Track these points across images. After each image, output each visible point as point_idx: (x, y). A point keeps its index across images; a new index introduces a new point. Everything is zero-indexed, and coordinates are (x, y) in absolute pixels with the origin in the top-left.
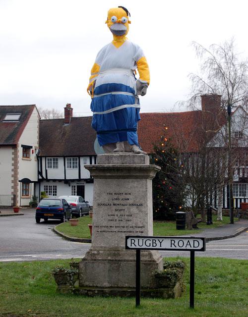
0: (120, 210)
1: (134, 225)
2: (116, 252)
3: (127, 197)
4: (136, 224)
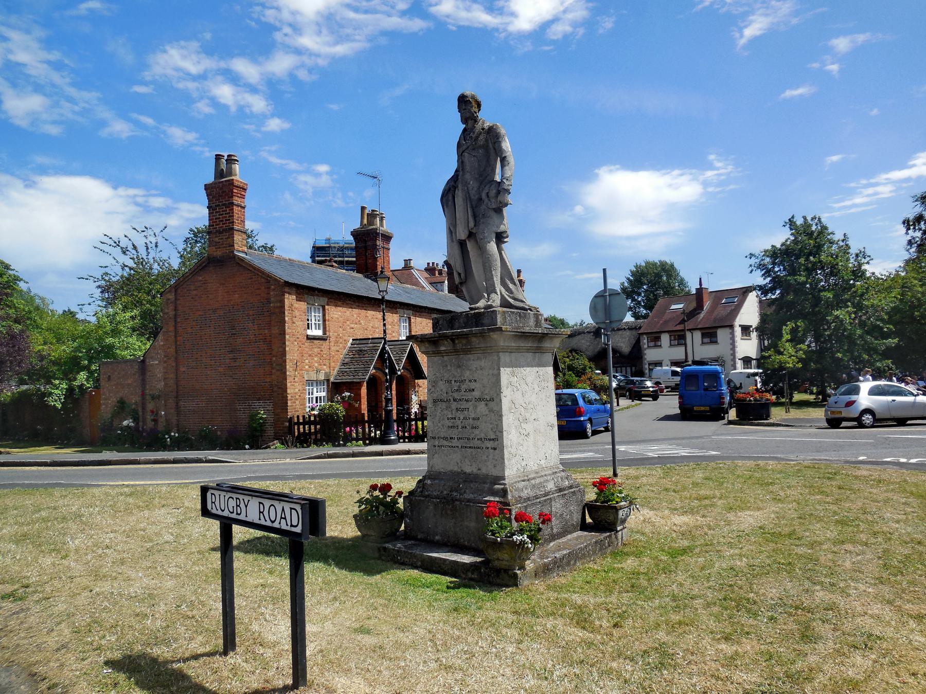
0: (463, 410)
1: (483, 436)
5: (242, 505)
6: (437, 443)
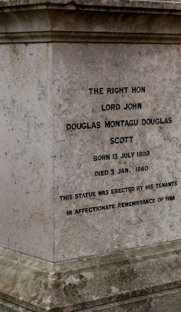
0: (124, 139)
1: (154, 181)
2: (124, 268)
4: (159, 176)
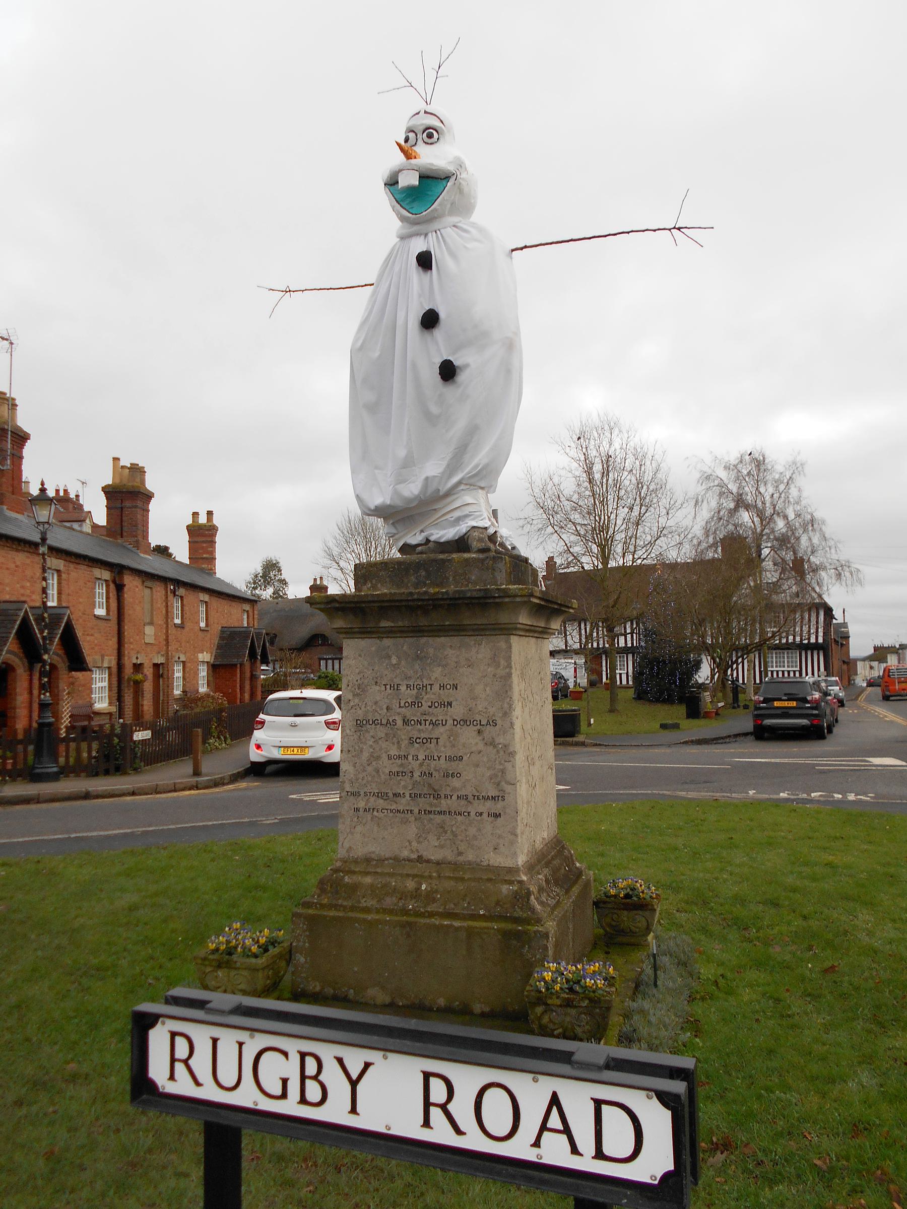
1: (469, 791)
3: (445, 695)
5: (333, 1076)
6: (362, 804)
